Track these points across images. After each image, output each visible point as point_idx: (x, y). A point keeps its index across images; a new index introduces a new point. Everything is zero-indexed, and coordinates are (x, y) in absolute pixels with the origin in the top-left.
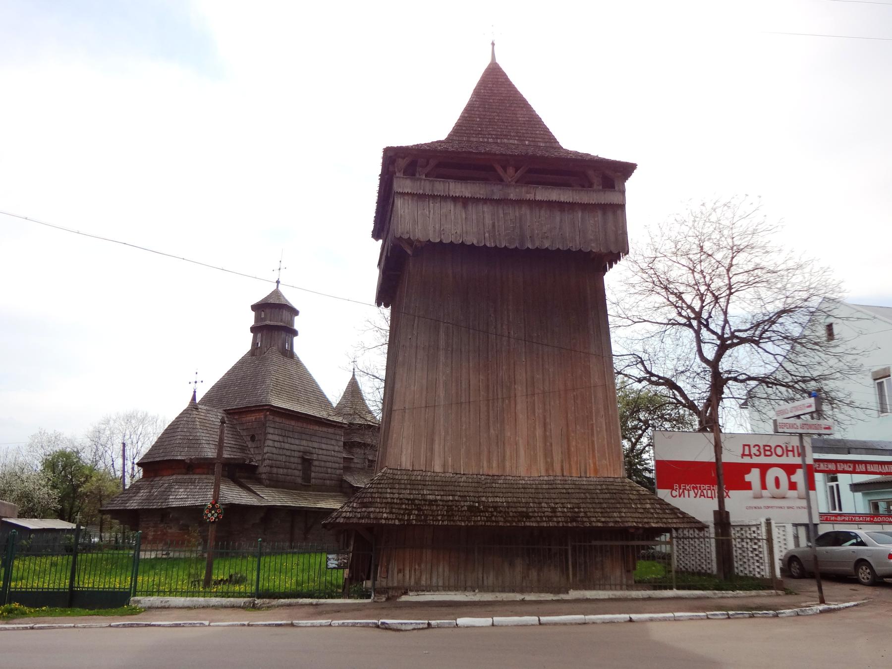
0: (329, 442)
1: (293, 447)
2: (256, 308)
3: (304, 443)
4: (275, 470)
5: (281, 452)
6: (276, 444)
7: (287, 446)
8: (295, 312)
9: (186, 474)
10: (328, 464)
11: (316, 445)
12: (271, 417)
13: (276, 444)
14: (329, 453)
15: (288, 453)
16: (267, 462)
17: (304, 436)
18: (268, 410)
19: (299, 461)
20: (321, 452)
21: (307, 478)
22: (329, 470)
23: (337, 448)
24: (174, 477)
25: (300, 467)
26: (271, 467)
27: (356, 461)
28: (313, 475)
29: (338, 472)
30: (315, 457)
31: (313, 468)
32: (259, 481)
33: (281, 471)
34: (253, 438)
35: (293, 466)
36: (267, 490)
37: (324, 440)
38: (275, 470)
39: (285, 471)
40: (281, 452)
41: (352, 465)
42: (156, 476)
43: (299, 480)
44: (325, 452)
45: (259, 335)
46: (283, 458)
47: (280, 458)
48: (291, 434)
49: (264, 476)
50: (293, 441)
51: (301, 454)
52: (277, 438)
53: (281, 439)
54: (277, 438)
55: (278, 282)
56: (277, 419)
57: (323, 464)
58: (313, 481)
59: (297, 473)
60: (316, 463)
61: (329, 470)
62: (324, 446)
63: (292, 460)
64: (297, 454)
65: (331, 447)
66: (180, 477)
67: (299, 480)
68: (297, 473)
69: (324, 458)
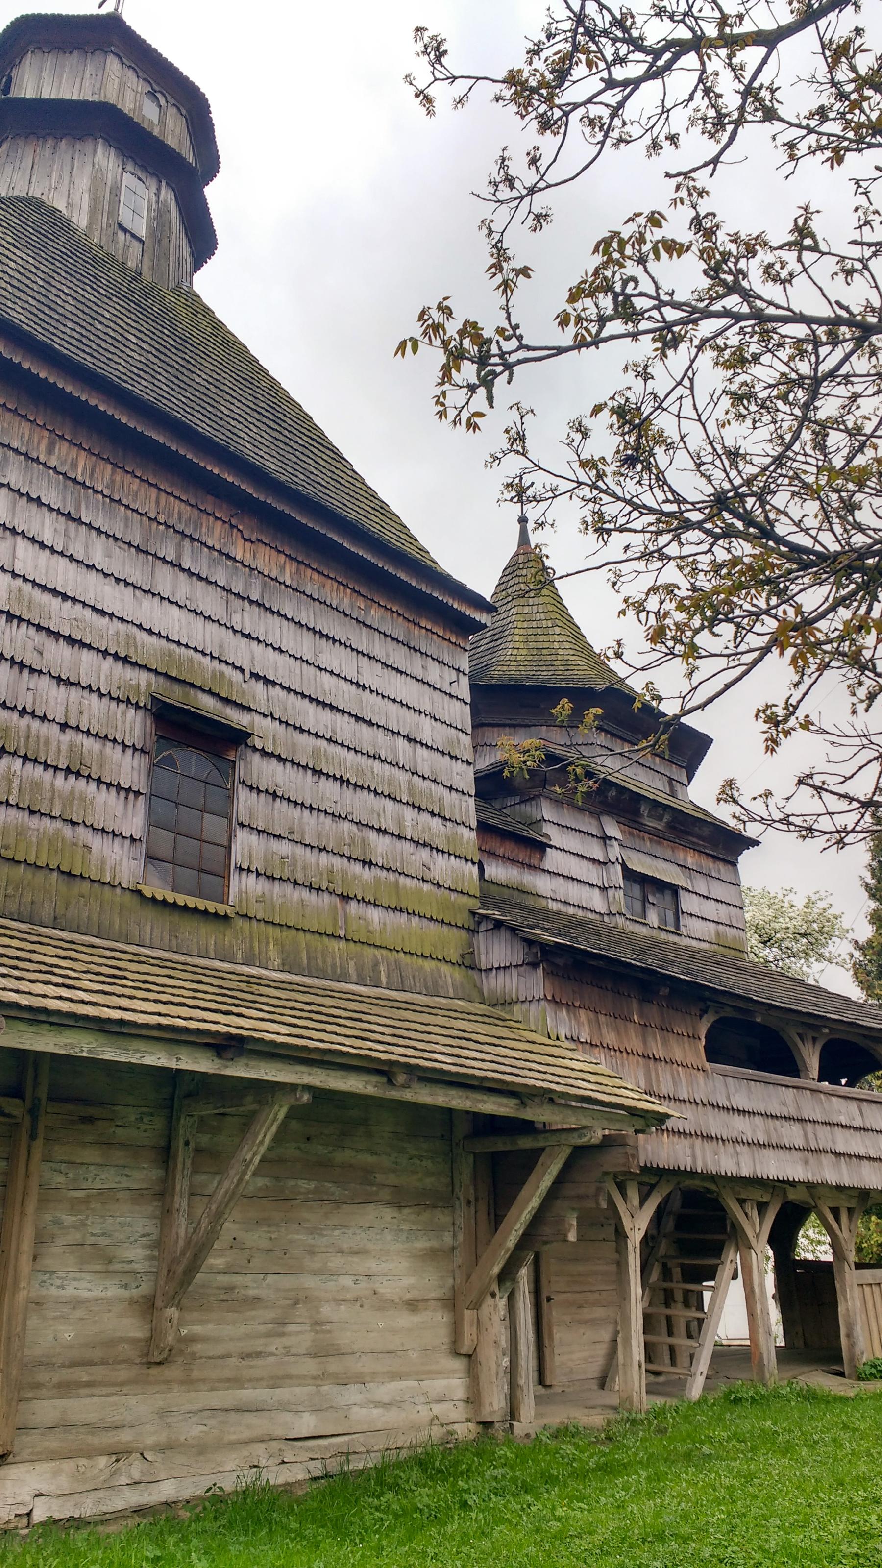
3: (172, 621)
17: (166, 581)
23: (427, 731)
25: (130, 769)
27: (553, 860)
28: (245, 845)
30: (265, 732)
37: (333, 657)
41: (542, 884)
43: (122, 863)
44: (345, 728)
57: (329, 792)
67: (122, 863)
68: (106, 806)
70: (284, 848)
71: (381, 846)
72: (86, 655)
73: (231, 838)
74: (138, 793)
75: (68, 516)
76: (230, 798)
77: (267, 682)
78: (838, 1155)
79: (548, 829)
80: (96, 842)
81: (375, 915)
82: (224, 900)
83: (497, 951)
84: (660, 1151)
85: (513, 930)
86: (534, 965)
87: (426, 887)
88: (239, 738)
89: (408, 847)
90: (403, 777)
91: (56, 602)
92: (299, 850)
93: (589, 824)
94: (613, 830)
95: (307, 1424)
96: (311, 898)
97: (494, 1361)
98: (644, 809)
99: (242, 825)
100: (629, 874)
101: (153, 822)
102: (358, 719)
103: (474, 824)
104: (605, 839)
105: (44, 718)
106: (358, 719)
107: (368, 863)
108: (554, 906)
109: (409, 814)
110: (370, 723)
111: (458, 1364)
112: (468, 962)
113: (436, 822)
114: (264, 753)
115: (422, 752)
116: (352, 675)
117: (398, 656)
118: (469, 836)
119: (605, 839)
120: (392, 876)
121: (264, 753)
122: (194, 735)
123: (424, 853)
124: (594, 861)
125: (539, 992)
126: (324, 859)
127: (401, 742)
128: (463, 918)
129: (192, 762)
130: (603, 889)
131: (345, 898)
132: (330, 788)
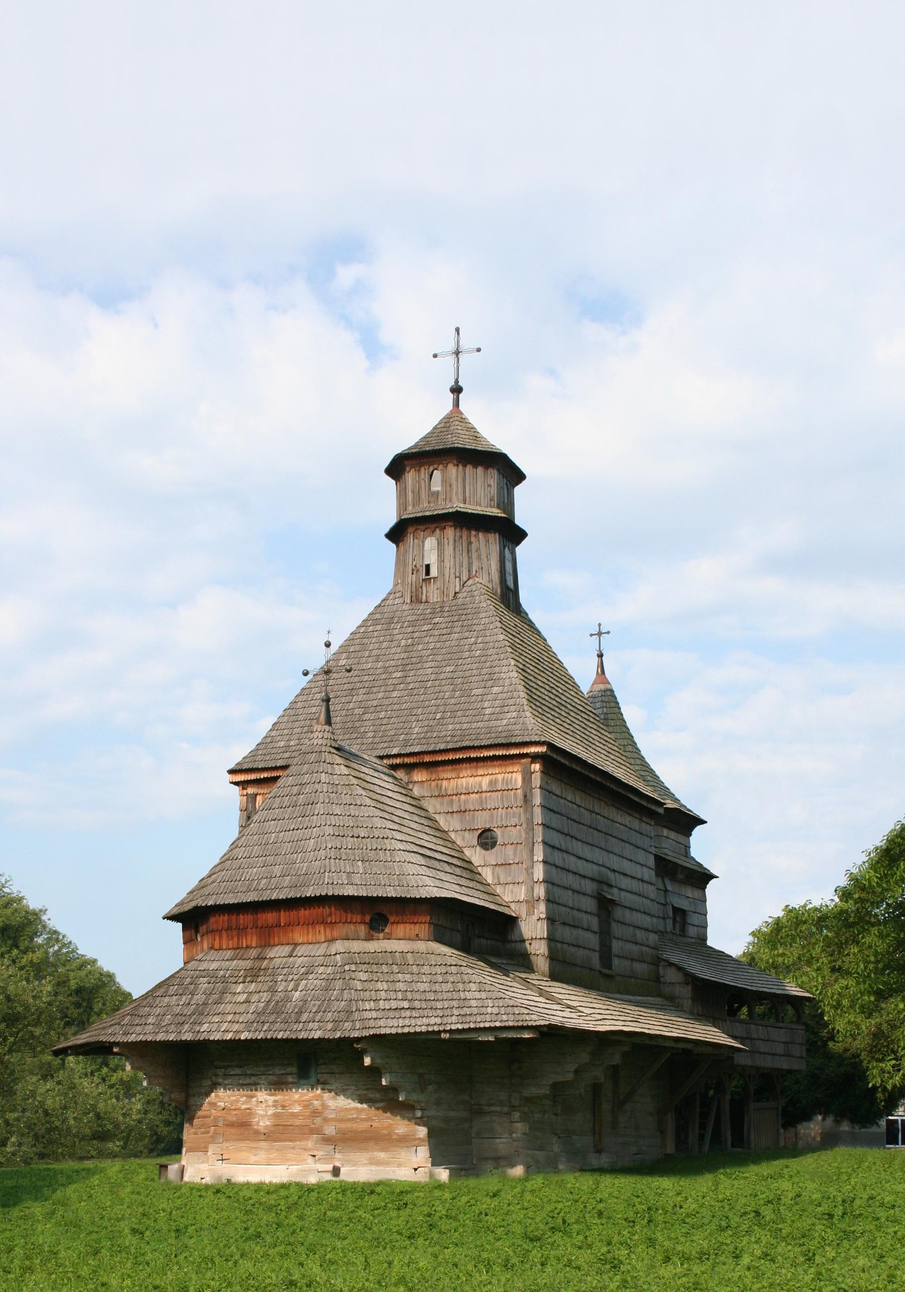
1: (582, 867)
2: (397, 468)
3: (598, 855)
9: (369, 938)
11: (614, 862)
14: (634, 885)
18: (535, 757)
20: (625, 882)
21: (606, 954)
22: (638, 932)
24: (339, 946)
25: (594, 922)
28: (616, 946)
31: (614, 925)
42: (266, 943)
45: (430, 543)
48: (574, 829)
55: (457, 390)
58: (616, 962)
60: (618, 913)
62: (627, 867)
64: (589, 887)
65: (638, 871)
66: (356, 946)
70: (620, 943)
71: (640, 935)
76: (610, 926)
77: (614, 871)
78: (761, 1053)
85: (679, 968)
86: (687, 984)
87: (648, 949)
88: (612, 902)
100: (676, 910)
107: (636, 943)
112: (658, 979)
122: (605, 906)
124: (662, 904)
125: (690, 995)
130: (664, 918)
132: (628, 912)
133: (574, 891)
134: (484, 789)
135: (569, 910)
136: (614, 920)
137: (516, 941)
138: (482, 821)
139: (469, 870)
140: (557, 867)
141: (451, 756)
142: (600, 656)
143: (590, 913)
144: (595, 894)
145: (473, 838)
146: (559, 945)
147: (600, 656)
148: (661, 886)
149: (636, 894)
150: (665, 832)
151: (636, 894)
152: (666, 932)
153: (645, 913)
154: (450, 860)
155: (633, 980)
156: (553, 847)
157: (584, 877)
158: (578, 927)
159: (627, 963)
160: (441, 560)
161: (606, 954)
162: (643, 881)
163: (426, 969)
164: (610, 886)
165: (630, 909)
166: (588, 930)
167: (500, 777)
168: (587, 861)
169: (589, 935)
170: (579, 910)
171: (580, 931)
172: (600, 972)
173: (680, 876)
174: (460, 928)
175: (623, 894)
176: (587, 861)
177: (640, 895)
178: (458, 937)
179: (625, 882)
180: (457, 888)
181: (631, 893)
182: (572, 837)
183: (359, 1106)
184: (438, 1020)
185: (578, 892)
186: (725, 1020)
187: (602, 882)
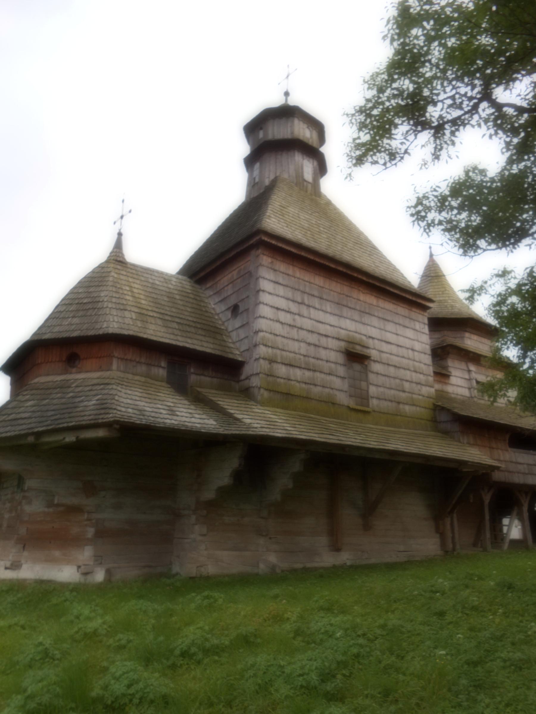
0: (400, 330)
1: (322, 329)
3: (348, 324)
4: (282, 370)
5: (294, 333)
6: (282, 316)
7: (307, 324)
8: (318, 127)
10: (402, 373)
11: (374, 332)
12: (265, 259)
13: (282, 316)
15: (312, 338)
16: (262, 350)
17: (346, 312)
19: (340, 358)
20: (385, 347)
23: (417, 346)
25: (341, 371)
26: (272, 361)
28: (373, 390)
29: (425, 390)
30: (374, 354)
31: (372, 377)
32: (246, 394)
33: (298, 373)
34: (235, 310)
35: (326, 367)
36: (258, 409)
37: (390, 327)
38: (282, 370)
39: (308, 374)
40: (294, 333)
41: (449, 389)
43: (343, 399)
45: (257, 166)
46: (303, 348)
47: (294, 346)
48: (316, 302)
49: (255, 382)
50: (321, 316)
51: (343, 344)
52: (282, 303)
53: (294, 307)
54: (282, 303)
56: (282, 266)
58: (374, 403)
59: (337, 382)
60: (376, 367)
61: (407, 385)
63: (323, 354)
65: (407, 343)
69: (395, 360)
70: (381, 389)
72: (330, 340)
73: (368, 388)
74: (345, 378)
75: (321, 298)
76: (367, 376)
77: (373, 338)
79: (451, 370)
80: (337, 393)
81: (407, 408)
82: (368, 406)
83: (444, 417)
84: (497, 476)
87: (420, 397)
89: (414, 385)
90: (411, 363)
91: (320, 325)
92: (386, 390)
93: (463, 365)
94: (472, 368)
95: (402, 548)
96: (390, 404)
97: (449, 534)
98: (482, 359)
99: (371, 384)
100: (478, 382)
101: (350, 386)
102: (398, 346)
103: (432, 374)
104: (469, 371)
105: (322, 360)
106: (398, 346)
107: (404, 391)
108: (453, 396)
109: (414, 374)
110: (401, 346)
111: (438, 535)
113: (421, 376)
114: (374, 361)
115: (416, 353)
116: (394, 331)
117: (407, 322)
118: (431, 379)
119: (469, 371)
120: (410, 395)
121: (374, 361)
123: (419, 386)
126: (393, 392)
127: (410, 351)
128: (431, 406)
129: (357, 367)
130: (469, 389)
131: (399, 403)
132: (392, 369)
133: (309, 344)
134: (235, 278)
135: (302, 357)
136: (373, 372)
137: (244, 380)
138: (232, 301)
139: (214, 331)
140: (282, 323)
141: (218, 263)
142: (430, 248)
143: (336, 363)
144: (343, 350)
145: (229, 314)
146: (282, 381)
147: (430, 248)
148: (466, 368)
149: (403, 357)
150: (467, 335)
151: (403, 357)
152: (472, 397)
153: (415, 371)
154: (191, 324)
155: (399, 417)
156: (278, 309)
157: (326, 336)
158: (315, 371)
159: (394, 404)
160: (261, 172)
161: (363, 397)
162: (413, 350)
163: (80, 389)
164: (368, 348)
165: (395, 366)
166: (330, 374)
167: (242, 267)
168: (331, 326)
169: (334, 379)
170: (318, 359)
171: (318, 374)
172: (348, 407)
173: (483, 362)
174: (163, 364)
175: (384, 356)
176: (331, 326)
177: (409, 359)
178: (162, 372)
179: (385, 347)
180: (172, 337)
181: (398, 356)
182: (309, 306)
183: (46, 510)
184: (33, 425)
185: (315, 345)
186: (507, 450)
187: (350, 342)
